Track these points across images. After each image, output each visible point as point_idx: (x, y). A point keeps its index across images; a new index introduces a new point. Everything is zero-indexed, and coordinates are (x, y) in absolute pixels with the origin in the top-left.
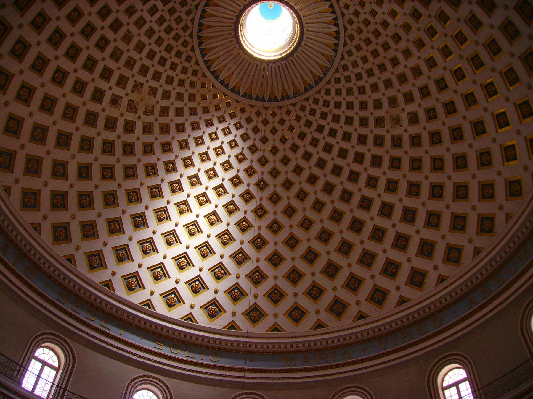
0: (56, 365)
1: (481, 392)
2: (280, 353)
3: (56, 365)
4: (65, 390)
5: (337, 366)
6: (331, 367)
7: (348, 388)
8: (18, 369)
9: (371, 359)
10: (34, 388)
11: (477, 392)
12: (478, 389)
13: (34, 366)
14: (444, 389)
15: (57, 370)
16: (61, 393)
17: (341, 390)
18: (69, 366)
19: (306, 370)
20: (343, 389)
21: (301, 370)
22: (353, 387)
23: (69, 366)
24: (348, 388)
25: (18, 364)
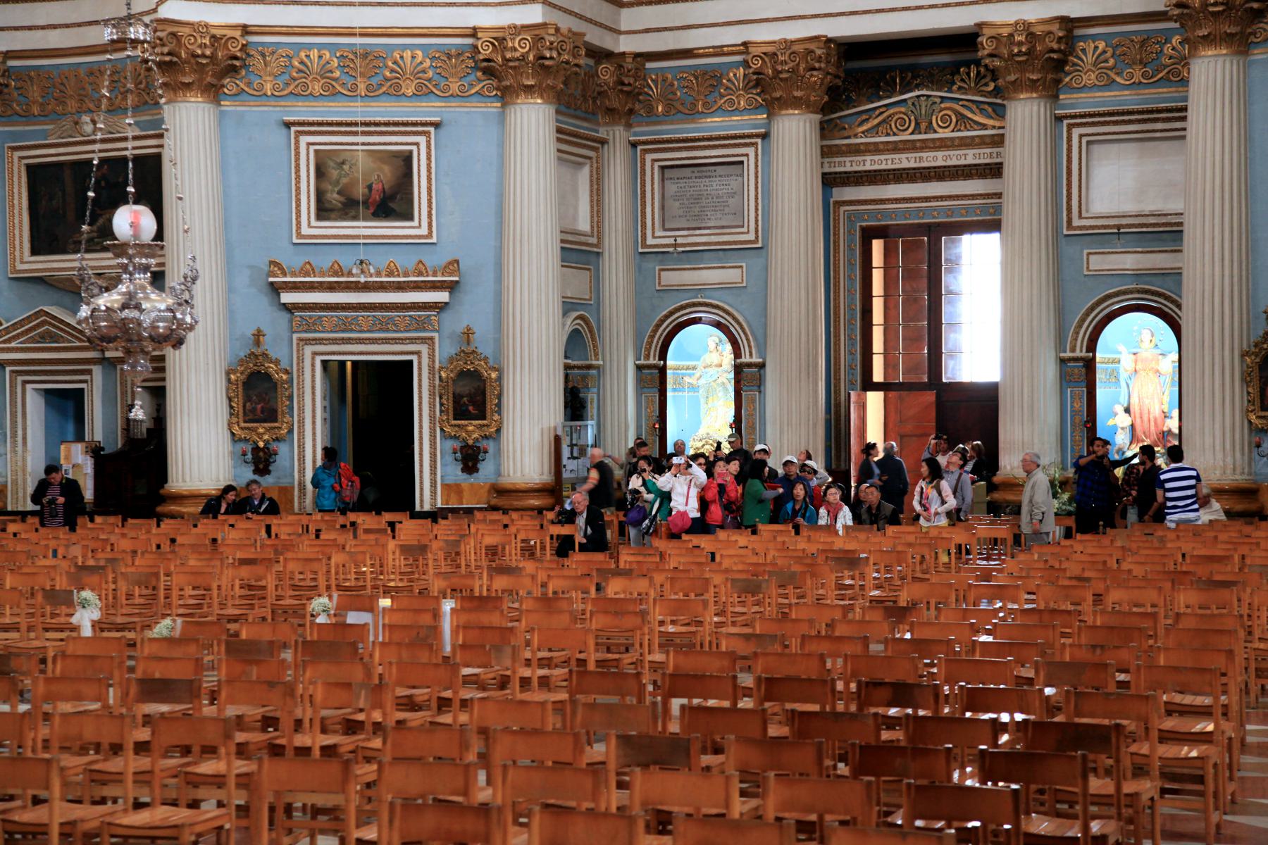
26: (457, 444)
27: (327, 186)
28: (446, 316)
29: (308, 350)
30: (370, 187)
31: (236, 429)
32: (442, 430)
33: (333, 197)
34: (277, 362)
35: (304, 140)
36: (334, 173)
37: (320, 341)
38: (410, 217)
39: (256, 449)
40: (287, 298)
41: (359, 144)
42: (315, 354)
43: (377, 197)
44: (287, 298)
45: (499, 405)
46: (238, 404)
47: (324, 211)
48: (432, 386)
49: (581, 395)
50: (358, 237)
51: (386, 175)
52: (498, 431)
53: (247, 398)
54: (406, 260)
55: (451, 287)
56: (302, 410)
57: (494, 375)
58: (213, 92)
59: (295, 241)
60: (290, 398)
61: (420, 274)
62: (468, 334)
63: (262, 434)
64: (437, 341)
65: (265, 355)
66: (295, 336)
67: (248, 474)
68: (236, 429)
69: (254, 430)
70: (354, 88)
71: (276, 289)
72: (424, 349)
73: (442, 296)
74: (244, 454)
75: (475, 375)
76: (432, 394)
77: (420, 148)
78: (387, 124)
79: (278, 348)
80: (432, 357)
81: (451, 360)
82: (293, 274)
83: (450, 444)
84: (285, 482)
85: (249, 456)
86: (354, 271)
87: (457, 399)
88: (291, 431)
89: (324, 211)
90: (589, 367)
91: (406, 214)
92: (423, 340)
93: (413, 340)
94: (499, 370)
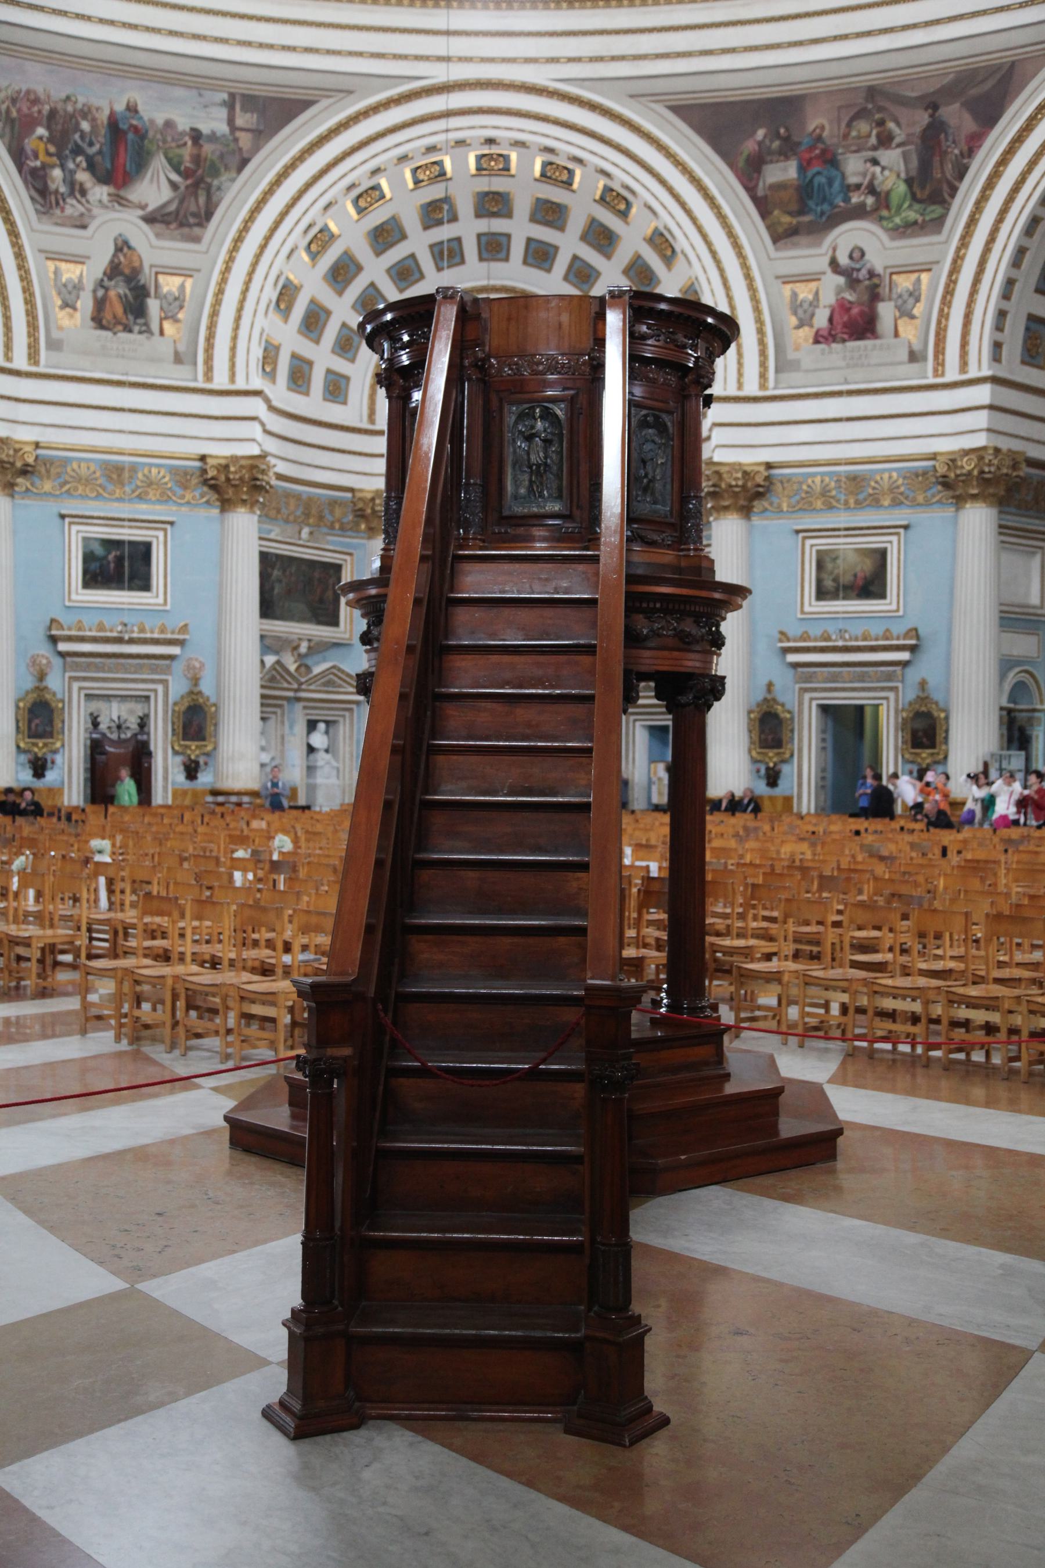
26: (30, 756)
27: (824, 576)
28: (909, 671)
29: (76, 686)
30: (855, 576)
31: (754, 753)
32: (903, 756)
33: (829, 583)
34: (783, 705)
35: (75, 528)
36: (829, 566)
37: (815, 690)
39: (768, 769)
41: (844, 544)
42: (812, 699)
43: (860, 582)
45: (946, 738)
46: (755, 736)
47: (822, 594)
48: (896, 723)
49: (1028, 732)
50: (837, 613)
51: (867, 566)
52: (946, 757)
53: (762, 732)
54: (876, 629)
55: (181, 643)
56: (800, 740)
57: (943, 715)
59: (67, 604)
60: (792, 731)
61: (887, 639)
62: (923, 684)
63: (40, 747)
64: (900, 689)
65: (774, 700)
66: (67, 675)
67: (26, 777)
68: (22, 745)
69: (765, 754)
70: (846, 503)
71: (54, 640)
72: (160, 688)
73: (904, 656)
74: (758, 771)
75: (928, 715)
76: (896, 731)
77: (893, 545)
78: (868, 528)
79: (788, 694)
80: (897, 701)
81: (910, 704)
82: (795, 641)
83: (179, 759)
84: (787, 793)
85: (763, 771)
86: (834, 637)
87: (914, 734)
88: (792, 755)
89: (822, 594)
90: (1034, 710)
91: (882, 596)
92: (891, 689)
93: (153, 681)
94: (946, 711)
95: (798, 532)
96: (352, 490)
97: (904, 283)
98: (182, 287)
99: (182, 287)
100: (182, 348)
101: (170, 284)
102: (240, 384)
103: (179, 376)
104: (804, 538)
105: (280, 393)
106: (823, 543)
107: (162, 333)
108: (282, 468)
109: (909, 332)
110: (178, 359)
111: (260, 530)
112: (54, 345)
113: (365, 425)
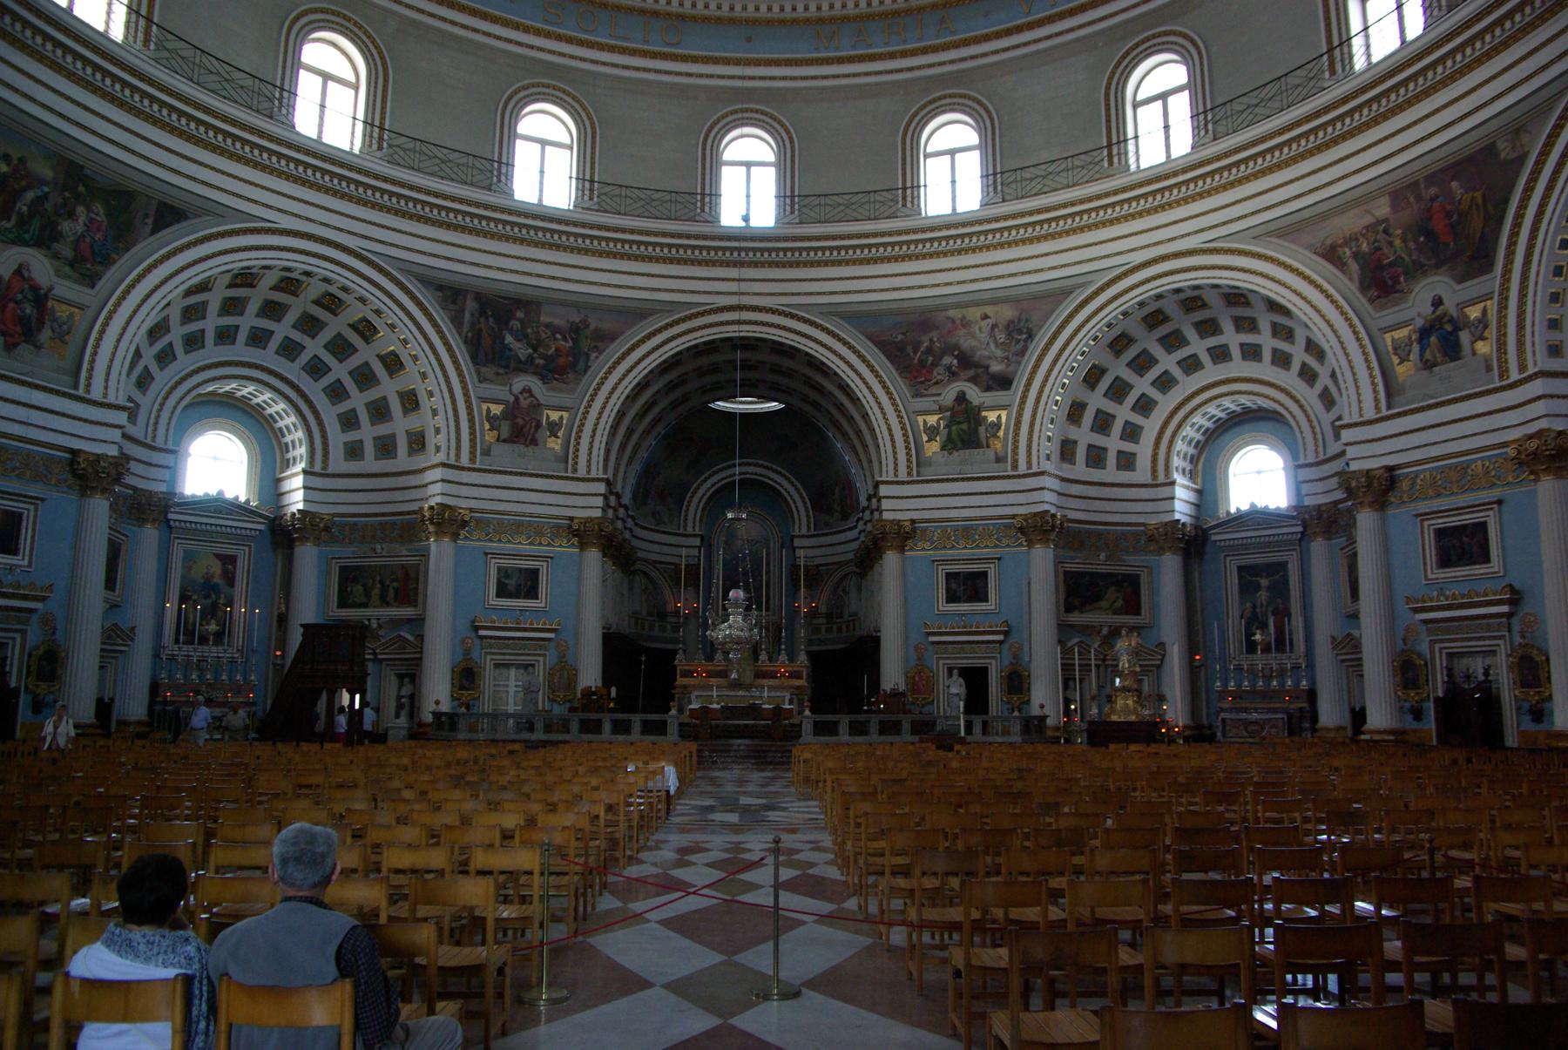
0: (353, 80)
1: (1210, 117)
2: (807, 21)
3: (353, 80)
4: (382, 128)
5: (925, 51)
6: (913, 53)
7: (945, 97)
8: (277, 95)
9: (998, 35)
10: (320, 132)
11: (1202, 117)
12: (1205, 112)
13: (307, 86)
14: (1136, 105)
15: (356, 88)
16: (376, 135)
17: (931, 102)
18: (377, 78)
19: (861, 59)
20: (934, 100)
21: (851, 60)
22: (955, 96)
23: (377, 78)
24: (945, 97)
25: (275, 86)
29: (941, 662)
38: (985, 600)
40: (932, 639)
44: (932, 639)
58: (901, 549)
72: (993, 662)
95: (1417, 516)
96: (1143, 524)
97: (1474, 313)
98: (999, 417)
99: (999, 417)
100: (1001, 454)
101: (992, 416)
102: (1035, 469)
103: (997, 470)
104: (1422, 520)
105: (1080, 469)
106: (1441, 522)
107: (988, 447)
108: (1073, 515)
109: (1483, 348)
110: (999, 459)
111: (1055, 556)
112: (929, 463)
113: (1149, 481)
